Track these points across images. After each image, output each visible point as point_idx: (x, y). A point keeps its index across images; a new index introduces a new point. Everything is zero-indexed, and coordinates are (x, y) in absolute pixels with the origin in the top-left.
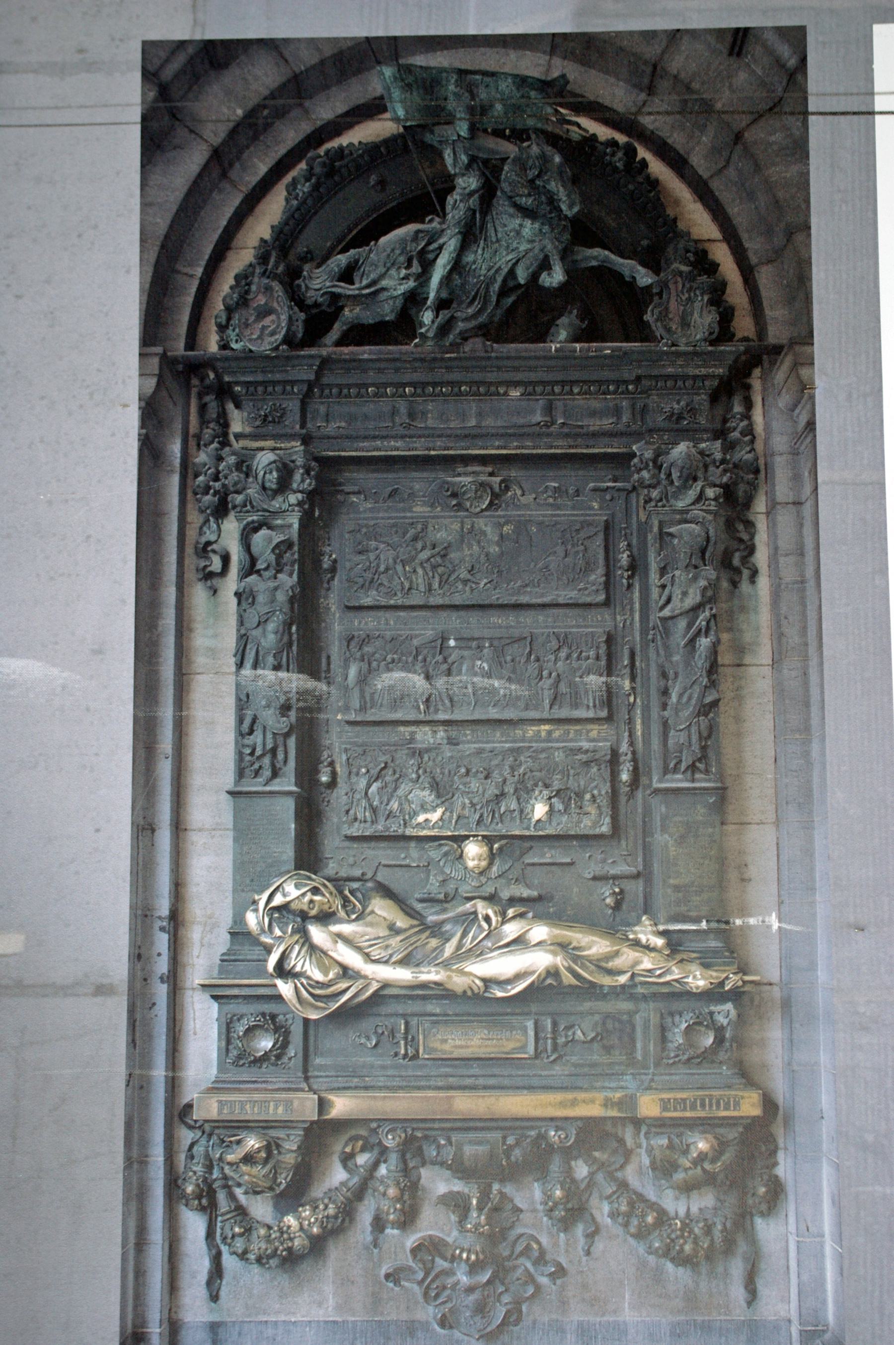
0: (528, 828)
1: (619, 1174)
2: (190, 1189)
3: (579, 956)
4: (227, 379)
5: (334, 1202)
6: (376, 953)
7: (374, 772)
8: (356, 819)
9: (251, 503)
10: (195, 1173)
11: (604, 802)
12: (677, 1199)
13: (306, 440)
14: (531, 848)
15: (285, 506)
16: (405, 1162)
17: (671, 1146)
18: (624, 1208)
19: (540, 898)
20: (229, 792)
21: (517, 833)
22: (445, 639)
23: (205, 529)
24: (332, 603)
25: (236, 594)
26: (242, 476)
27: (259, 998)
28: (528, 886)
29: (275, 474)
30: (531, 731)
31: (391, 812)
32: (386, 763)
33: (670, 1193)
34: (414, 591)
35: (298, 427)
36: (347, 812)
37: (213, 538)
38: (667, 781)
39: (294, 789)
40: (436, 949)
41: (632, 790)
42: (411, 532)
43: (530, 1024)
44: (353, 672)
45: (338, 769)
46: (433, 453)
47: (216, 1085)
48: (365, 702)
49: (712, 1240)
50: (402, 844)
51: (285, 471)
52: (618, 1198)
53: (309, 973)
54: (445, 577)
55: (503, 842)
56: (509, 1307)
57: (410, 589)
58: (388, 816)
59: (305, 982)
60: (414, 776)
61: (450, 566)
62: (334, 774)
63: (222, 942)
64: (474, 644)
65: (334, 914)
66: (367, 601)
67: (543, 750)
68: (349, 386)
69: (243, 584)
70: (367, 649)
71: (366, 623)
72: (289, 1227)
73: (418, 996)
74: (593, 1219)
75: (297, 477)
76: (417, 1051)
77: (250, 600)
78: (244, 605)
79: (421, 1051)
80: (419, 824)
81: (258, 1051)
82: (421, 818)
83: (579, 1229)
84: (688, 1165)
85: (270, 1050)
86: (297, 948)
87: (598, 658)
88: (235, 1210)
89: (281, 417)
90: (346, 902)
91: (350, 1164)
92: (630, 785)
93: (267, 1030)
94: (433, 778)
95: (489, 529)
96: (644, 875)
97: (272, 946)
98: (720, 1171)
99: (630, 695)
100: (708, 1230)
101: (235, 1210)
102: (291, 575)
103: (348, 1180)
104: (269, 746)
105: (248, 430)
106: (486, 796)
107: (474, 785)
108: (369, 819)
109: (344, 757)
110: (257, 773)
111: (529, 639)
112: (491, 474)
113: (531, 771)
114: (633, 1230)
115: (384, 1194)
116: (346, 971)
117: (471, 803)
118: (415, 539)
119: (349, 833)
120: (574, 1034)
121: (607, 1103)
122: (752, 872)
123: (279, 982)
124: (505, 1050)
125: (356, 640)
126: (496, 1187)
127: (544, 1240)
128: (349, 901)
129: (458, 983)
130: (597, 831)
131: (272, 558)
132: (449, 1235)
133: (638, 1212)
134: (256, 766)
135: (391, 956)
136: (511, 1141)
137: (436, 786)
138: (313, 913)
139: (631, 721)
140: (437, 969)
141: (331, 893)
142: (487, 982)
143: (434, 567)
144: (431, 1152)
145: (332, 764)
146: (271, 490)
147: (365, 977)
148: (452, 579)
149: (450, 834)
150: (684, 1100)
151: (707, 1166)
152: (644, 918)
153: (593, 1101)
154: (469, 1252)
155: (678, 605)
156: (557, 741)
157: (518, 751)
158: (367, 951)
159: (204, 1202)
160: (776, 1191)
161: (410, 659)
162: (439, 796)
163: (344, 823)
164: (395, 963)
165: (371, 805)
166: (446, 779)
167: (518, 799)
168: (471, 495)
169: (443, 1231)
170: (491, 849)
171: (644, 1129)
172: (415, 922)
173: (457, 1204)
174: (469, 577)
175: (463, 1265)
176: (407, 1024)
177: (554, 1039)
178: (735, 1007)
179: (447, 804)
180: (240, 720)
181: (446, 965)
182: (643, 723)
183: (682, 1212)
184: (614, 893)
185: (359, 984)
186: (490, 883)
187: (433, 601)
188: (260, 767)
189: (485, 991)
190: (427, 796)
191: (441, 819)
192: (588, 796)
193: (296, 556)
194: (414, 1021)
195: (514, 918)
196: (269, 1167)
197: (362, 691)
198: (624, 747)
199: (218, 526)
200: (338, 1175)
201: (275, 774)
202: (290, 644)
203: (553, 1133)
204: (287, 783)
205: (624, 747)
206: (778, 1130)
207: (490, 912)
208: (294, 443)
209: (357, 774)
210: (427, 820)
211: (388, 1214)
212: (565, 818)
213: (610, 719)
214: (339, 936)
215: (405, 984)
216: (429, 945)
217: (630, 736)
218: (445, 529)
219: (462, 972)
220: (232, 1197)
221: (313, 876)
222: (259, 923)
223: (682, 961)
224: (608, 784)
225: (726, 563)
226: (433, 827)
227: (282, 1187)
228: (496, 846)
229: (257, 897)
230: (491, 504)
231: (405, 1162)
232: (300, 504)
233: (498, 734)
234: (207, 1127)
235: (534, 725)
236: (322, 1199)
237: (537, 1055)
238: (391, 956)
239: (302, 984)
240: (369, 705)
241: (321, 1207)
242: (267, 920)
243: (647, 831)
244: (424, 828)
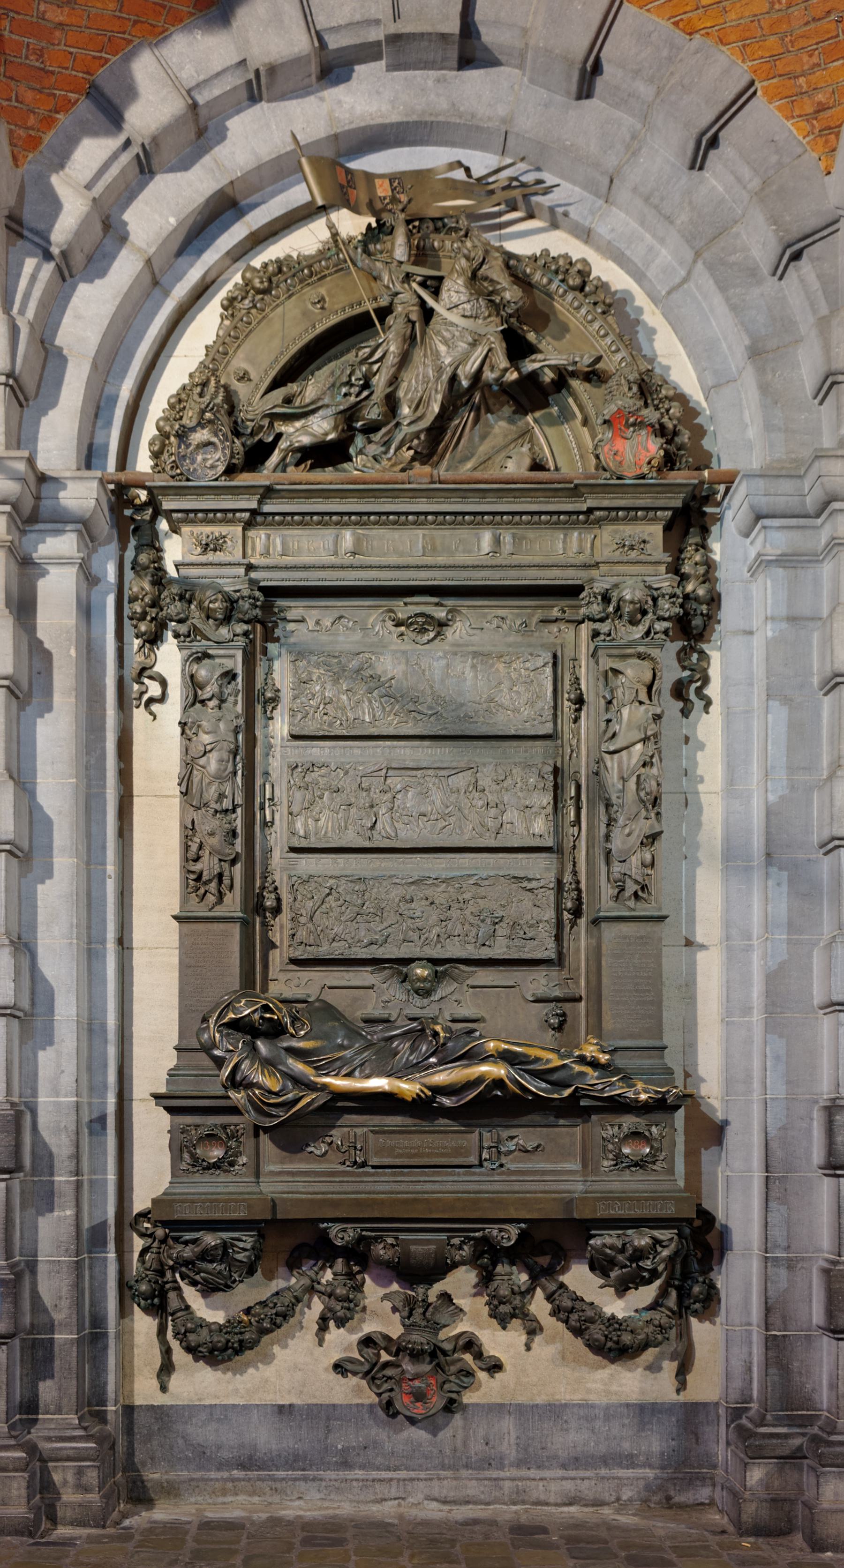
20: (175, 917)
25: (180, 723)
62: (279, 900)
134: (202, 891)
180: (187, 848)
188: (206, 892)
225: (679, 691)
230: (438, 634)
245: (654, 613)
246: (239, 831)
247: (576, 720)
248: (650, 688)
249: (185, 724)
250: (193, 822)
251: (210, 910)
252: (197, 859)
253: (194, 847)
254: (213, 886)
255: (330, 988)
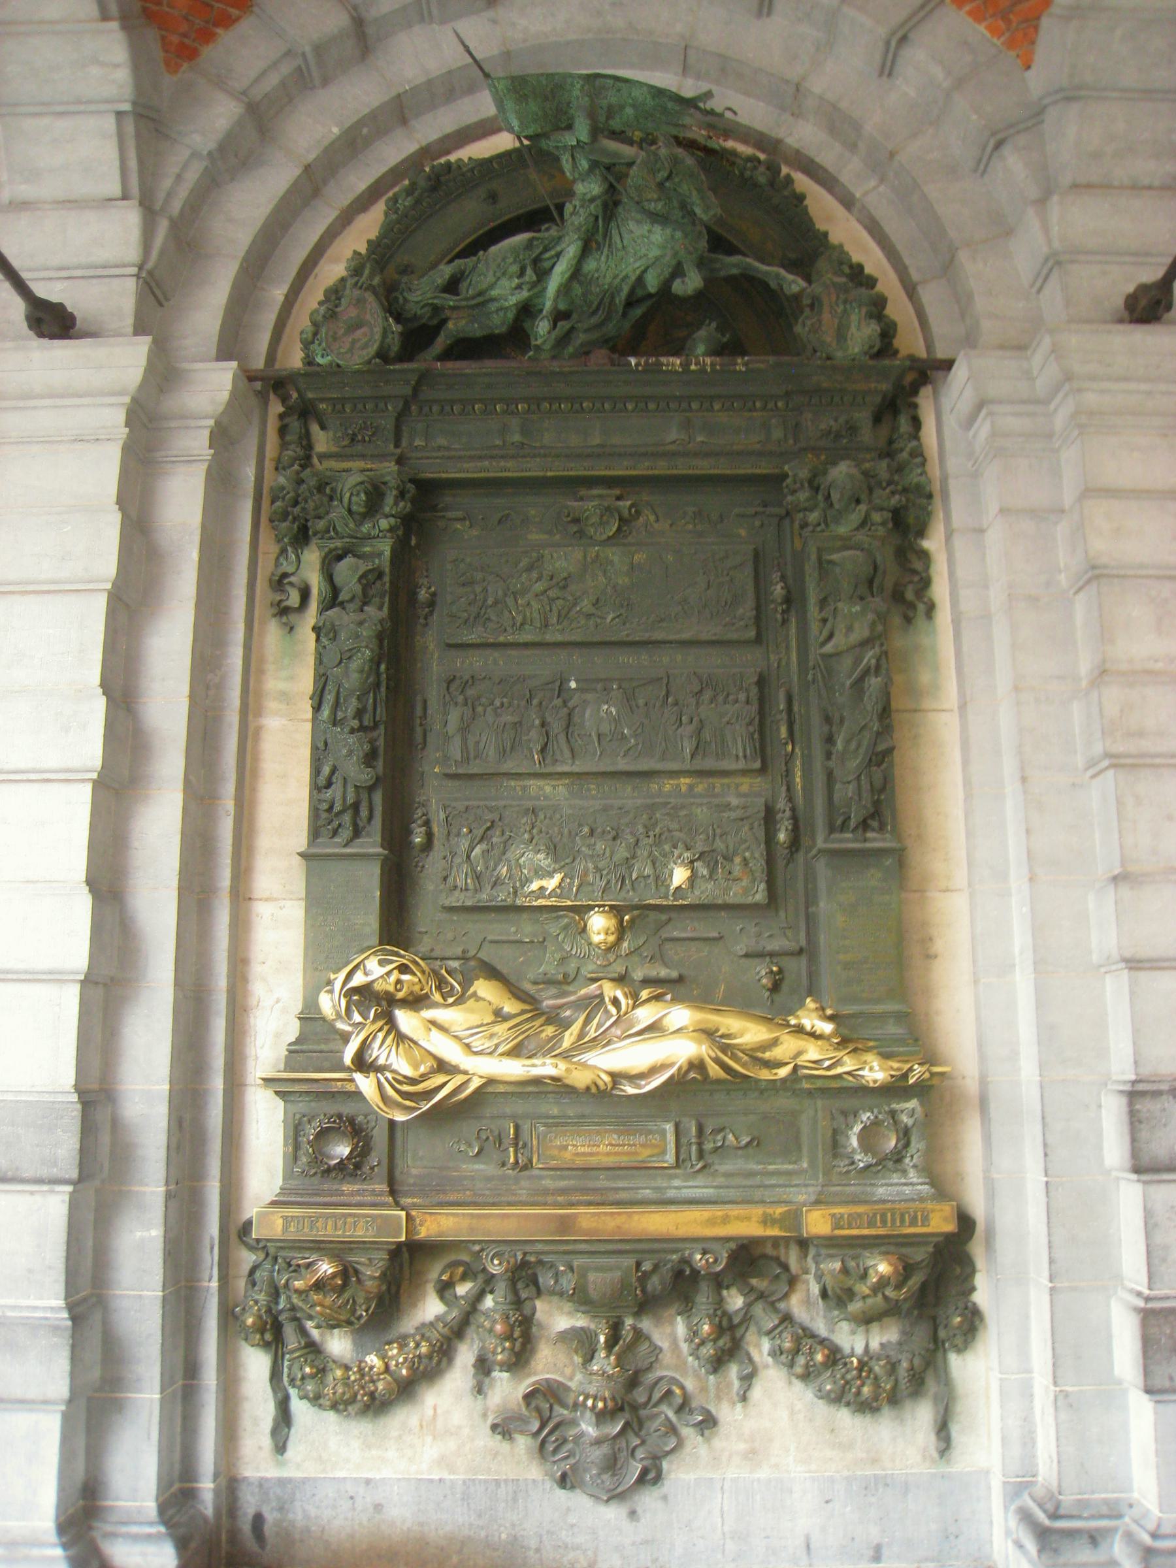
0: (666, 897)
1: (782, 1306)
2: (250, 1321)
3: (729, 1045)
4: (310, 395)
5: (428, 1340)
6: (478, 1043)
7: (479, 832)
8: (456, 887)
9: (334, 528)
10: (256, 1302)
11: (758, 865)
12: (853, 1333)
13: (400, 461)
14: (670, 920)
15: (375, 532)
16: (516, 1293)
17: (845, 1270)
18: (787, 1345)
19: (681, 979)
20: (300, 854)
21: (652, 902)
22: (563, 682)
23: (282, 559)
24: (430, 641)
26: (325, 499)
27: (333, 1095)
28: (666, 965)
29: (363, 496)
30: (668, 785)
31: (498, 878)
32: (493, 822)
33: (845, 1326)
34: (527, 627)
35: (392, 446)
36: (445, 879)
37: (290, 569)
38: (833, 841)
39: (380, 850)
40: (551, 1039)
41: (792, 853)
42: (525, 562)
43: (669, 1127)
44: (454, 717)
45: (435, 829)
46: (549, 474)
47: (282, 1199)
48: (468, 753)
49: (896, 1381)
50: (512, 916)
51: (375, 495)
52: (781, 1332)
53: (394, 1067)
54: (563, 613)
55: (636, 913)
56: (646, 1463)
57: (522, 624)
58: (495, 883)
59: (389, 1075)
60: (526, 836)
61: (570, 598)
62: (429, 836)
63: (293, 1030)
64: (599, 686)
65: (427, 996)
66: (472, 638)
67: (683, 807)
68: (452, 402)
69: (323, 617)
70: (470, 692)
71: (471, 664)
72: (372, 1368)
73: (529, 1093)
74: (750, 1359)
75: (389, 500)
76: (531, 1161)
77: (332, 635)
78: (324, 640)
79: (535, 1160)
80: (533, 892)
81: (333, 1158)
82: (535, 886)
83: (733, 1370)
84: (867, 1291)
85: (348, 1158)
86: (381, 1035)
87: (748, 702)
88: (305, 1347)
89: (374, 434)
90: (441, 984)
91: (447, 1295)
92: (790, 847)
93: (344, 1133)
94: (550, 838)
95: (616, 559)
96: (808, 951)
97: (349, 1034)
98: (905, 1300)
99: (787, 743)
100: (893, 1367)
101: (305, 1347)
102: (380, 608)
103: (446, 1313)
104: (350, 799)
105: (334, 449)
106: (615, 858)
107: (600, 846)
108: (471, 886)
109: (442, 816)
110: (335, 833)
111: (665, 681)
112: (619, 498)
113: (669, 831)
114: (799, 1370)
115: (491, 1330)
116: (442, 1066)
117: (596, 868)
118: (530, 568)
119: (447, 903)
120: (724, 1138)
121: (766, 1221)
122: (939, 946)
123: (358, 1077)
124: (640, 1158)
125: (458, 682)
126: (629, 1322)
127: (690, 1384)
128: (447, 983)
129: (580, 1079)
130: (750, 900)
131: (358, 589)
132: (571, 1379)
133: (806, 1349)
135: (497, 1046)
136: (647, 1266)
137: (553, 850)
138: (400, 995)
139: (788, 774)
140: (554, 1061)
141: (423, 972)
142: (617, 1077)
143: (552, 600)
144: (546, 1280)
145: (427, 823)
146: (359, 514)
147: (465, 1073)
148: (572, 613)
149: (569, 903)
150: (859, 1215)
151: (890, 1292)
152: (808, 1000)
153: (748, 1218)
154: (595, 1398)
155: (840, 641)
156: (701, 796)
157: (652, 808)
158: (466, 1041)
159: (268, 1337)
160: (973, 1321)
161: (523, 703)
162: (556, 861)
163: (441, 891)
164: (502, 1054)
165: (474, 870)
166: (565, 840)
167: (654, 864)
168: (595, 519)
169: (562, 1374)
170: (622, 921)
171: (812, 1251)
172: (527, 1007)
173: (582, 1342)
174: (593, 610)
175: (588, 1414)
176: (517, 1128)
177: (700, 1144)
178: (922, 1104)
179: (566, 869)
180: (316, 771)
181: (566, 1056)
182: (803, 777)
183: (859, 1349)
184: (772, 972)
185: (458, 1080)
186: (619, 961)
187: (549, 638)
188: (340, 825)
189: (613, 1088)
190: (542, 860)
191: (560, 886)
192: (737, 860)
193: (387, 586)
194: (526, 1127)
195: (648, 1000)
196: (346, 1295)
197: (465, 742)
198: (781, 804)
199: (298, 558)
200: (431, 1308)
201: (357, 833)
202: (377, 685)
203: (699, 1257)
204: (372, 844)
205: (781, 804)
206: (977, 1249)
207: (619, 994)
208: (387, 464)
209: (458, 835)
210: (542, 888)
211: (494, 1353)
212: (710, 885)
213: (763, 770)
214: (433, 1023)
215: (512, 1079)
216: (543, 1035)
217: (788, 790)
218: (564, 559)
219: (584, 1065)
220: (303, 1332)
221: (402, 952)
222: (334, 1006)
223: (855, 1050)
224: (763, 846)
226: (550, 896)
227: (362, 1321)
228: (627, 917)
229: (332, 976)
230: (619, 529)
231: (516, 1293)
232: (391, 529)
233: (629, 789)
234: (272, 1251)
235: (671, 778)
236: (413, 1336)
237: (678, 1163)
238: (497, 1046)
239: (387, 1079)
240: (472, 756)
241: (412, 1344)
242: (343, 1002)
243: (811, 899)
244: (538, 898)
245: (870, 502)
246: (381, 751)
247: (785, 622)
248: (871, 582)
249: (320, 628)
250: (326, 744)
251: (345, 846)
252: (329, 785)
253: (326, 770)
254: (347, 818)
255: (491, 942)
